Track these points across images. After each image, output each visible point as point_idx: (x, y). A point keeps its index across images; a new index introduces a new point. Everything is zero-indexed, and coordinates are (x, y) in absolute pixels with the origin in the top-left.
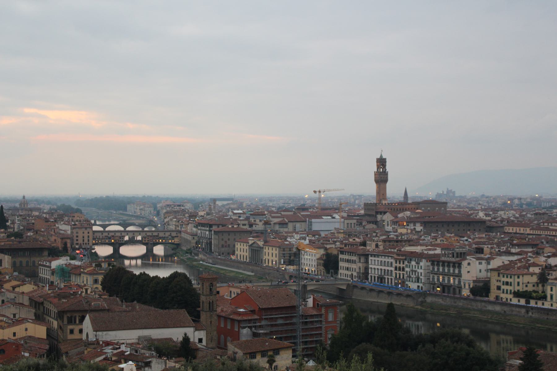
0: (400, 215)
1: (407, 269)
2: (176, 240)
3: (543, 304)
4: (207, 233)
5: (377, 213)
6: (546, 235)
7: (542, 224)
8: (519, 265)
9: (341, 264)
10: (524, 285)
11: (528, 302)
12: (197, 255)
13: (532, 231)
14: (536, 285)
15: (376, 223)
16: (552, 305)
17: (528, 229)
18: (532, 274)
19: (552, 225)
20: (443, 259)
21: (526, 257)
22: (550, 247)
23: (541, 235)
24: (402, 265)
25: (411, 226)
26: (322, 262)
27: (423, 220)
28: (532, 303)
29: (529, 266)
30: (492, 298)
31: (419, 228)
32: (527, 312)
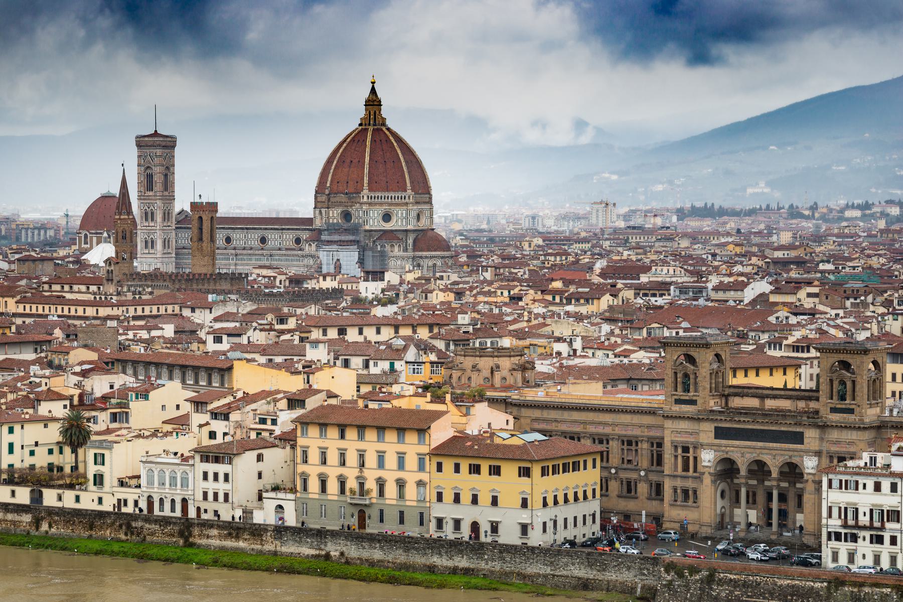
3: (78, 499)
6: (59, 316)
7: (46, 287)
8: (11, 397)
10: (27, 451)
11: (37, 497)
13: (21, 306)
14: (56, 450)
16: (100, 499)
17: (11, 302)
18: (46, 421)
19: (71, 291)
21: (27, 375)
22: (85, 346)
23: (47, 316)
28: (50, 498)
29: (39, 401)
32: (37, 523)
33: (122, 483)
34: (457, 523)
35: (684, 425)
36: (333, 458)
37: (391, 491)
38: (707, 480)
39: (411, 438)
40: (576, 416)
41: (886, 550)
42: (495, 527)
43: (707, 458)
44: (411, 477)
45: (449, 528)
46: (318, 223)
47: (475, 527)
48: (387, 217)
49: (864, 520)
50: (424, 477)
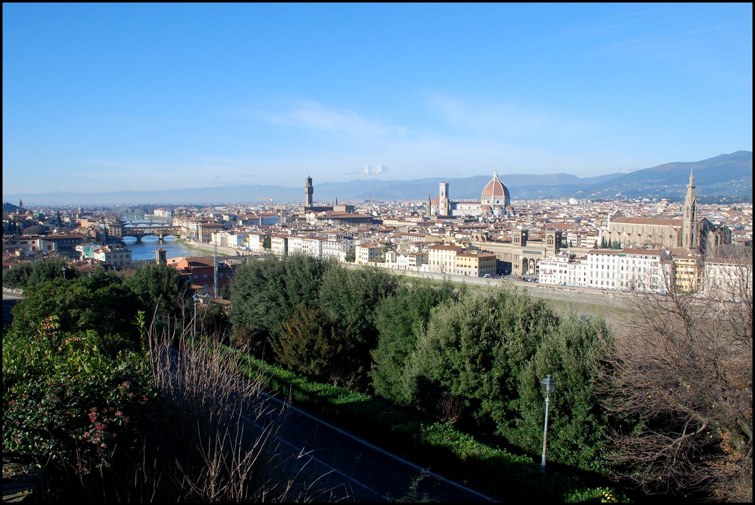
0: (319, 215)
1: (309, 247)
2: (179, 233)
4: (196, 227)
5: (305, 213)
9: (273, 245)
12: (190, 241)
15: (305, 219)
17: (397, 221)
20: (329, 240)
24: (306, 245)
25: (326, 221)
26: (262, 244)
27: (333, 217)
30: (356, 262)
31: (330, 222)
33: (393, 262)
34: (462, 272)
35: (516, 250)
36: (436, 256)
37: (448, 264)
38: (521, 262)
39: (452, 252)
40: (495, 248)
41: (553, 279)
42: (470, 273)
43: (521, 258)
44: (452, 261)
45: (460, 272)
46: (482, 203)
47: (465, 272)
48: (498, 202)
49: (548, 272)
50: (455, 261)
